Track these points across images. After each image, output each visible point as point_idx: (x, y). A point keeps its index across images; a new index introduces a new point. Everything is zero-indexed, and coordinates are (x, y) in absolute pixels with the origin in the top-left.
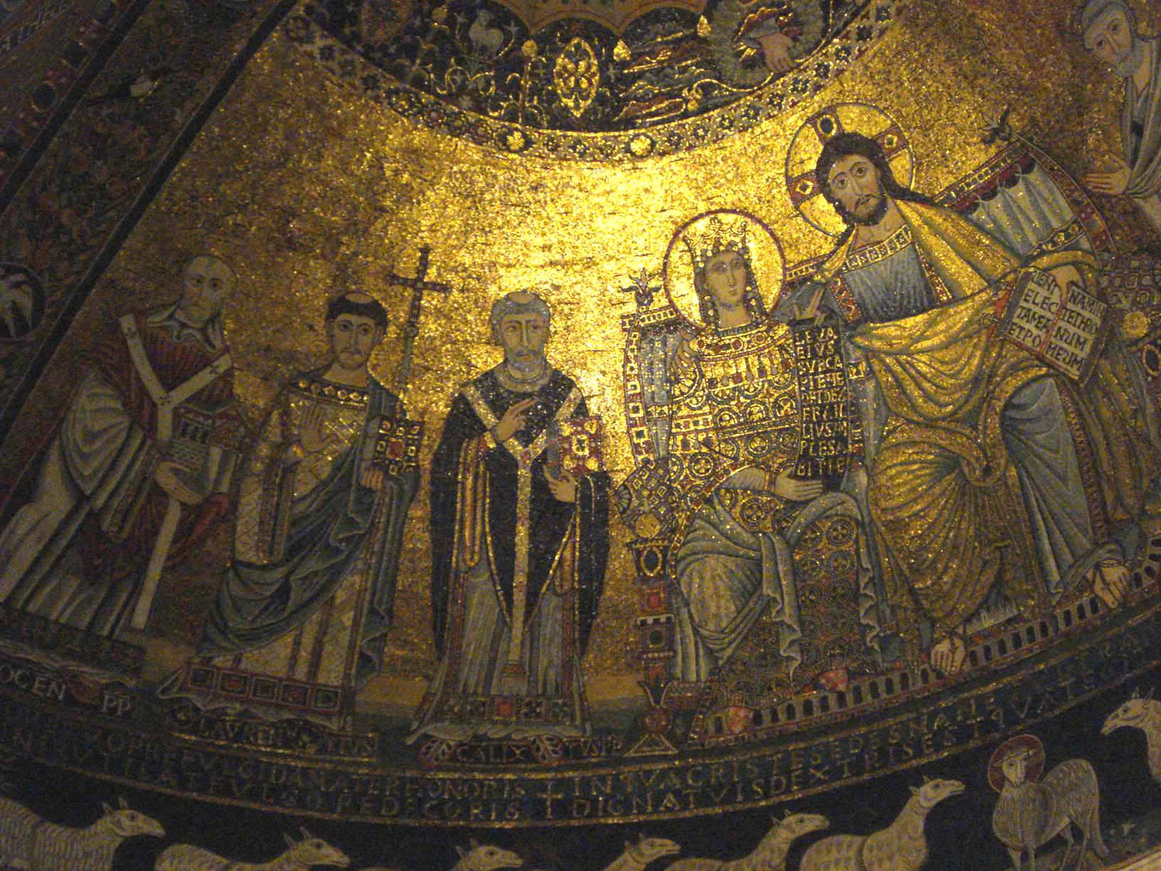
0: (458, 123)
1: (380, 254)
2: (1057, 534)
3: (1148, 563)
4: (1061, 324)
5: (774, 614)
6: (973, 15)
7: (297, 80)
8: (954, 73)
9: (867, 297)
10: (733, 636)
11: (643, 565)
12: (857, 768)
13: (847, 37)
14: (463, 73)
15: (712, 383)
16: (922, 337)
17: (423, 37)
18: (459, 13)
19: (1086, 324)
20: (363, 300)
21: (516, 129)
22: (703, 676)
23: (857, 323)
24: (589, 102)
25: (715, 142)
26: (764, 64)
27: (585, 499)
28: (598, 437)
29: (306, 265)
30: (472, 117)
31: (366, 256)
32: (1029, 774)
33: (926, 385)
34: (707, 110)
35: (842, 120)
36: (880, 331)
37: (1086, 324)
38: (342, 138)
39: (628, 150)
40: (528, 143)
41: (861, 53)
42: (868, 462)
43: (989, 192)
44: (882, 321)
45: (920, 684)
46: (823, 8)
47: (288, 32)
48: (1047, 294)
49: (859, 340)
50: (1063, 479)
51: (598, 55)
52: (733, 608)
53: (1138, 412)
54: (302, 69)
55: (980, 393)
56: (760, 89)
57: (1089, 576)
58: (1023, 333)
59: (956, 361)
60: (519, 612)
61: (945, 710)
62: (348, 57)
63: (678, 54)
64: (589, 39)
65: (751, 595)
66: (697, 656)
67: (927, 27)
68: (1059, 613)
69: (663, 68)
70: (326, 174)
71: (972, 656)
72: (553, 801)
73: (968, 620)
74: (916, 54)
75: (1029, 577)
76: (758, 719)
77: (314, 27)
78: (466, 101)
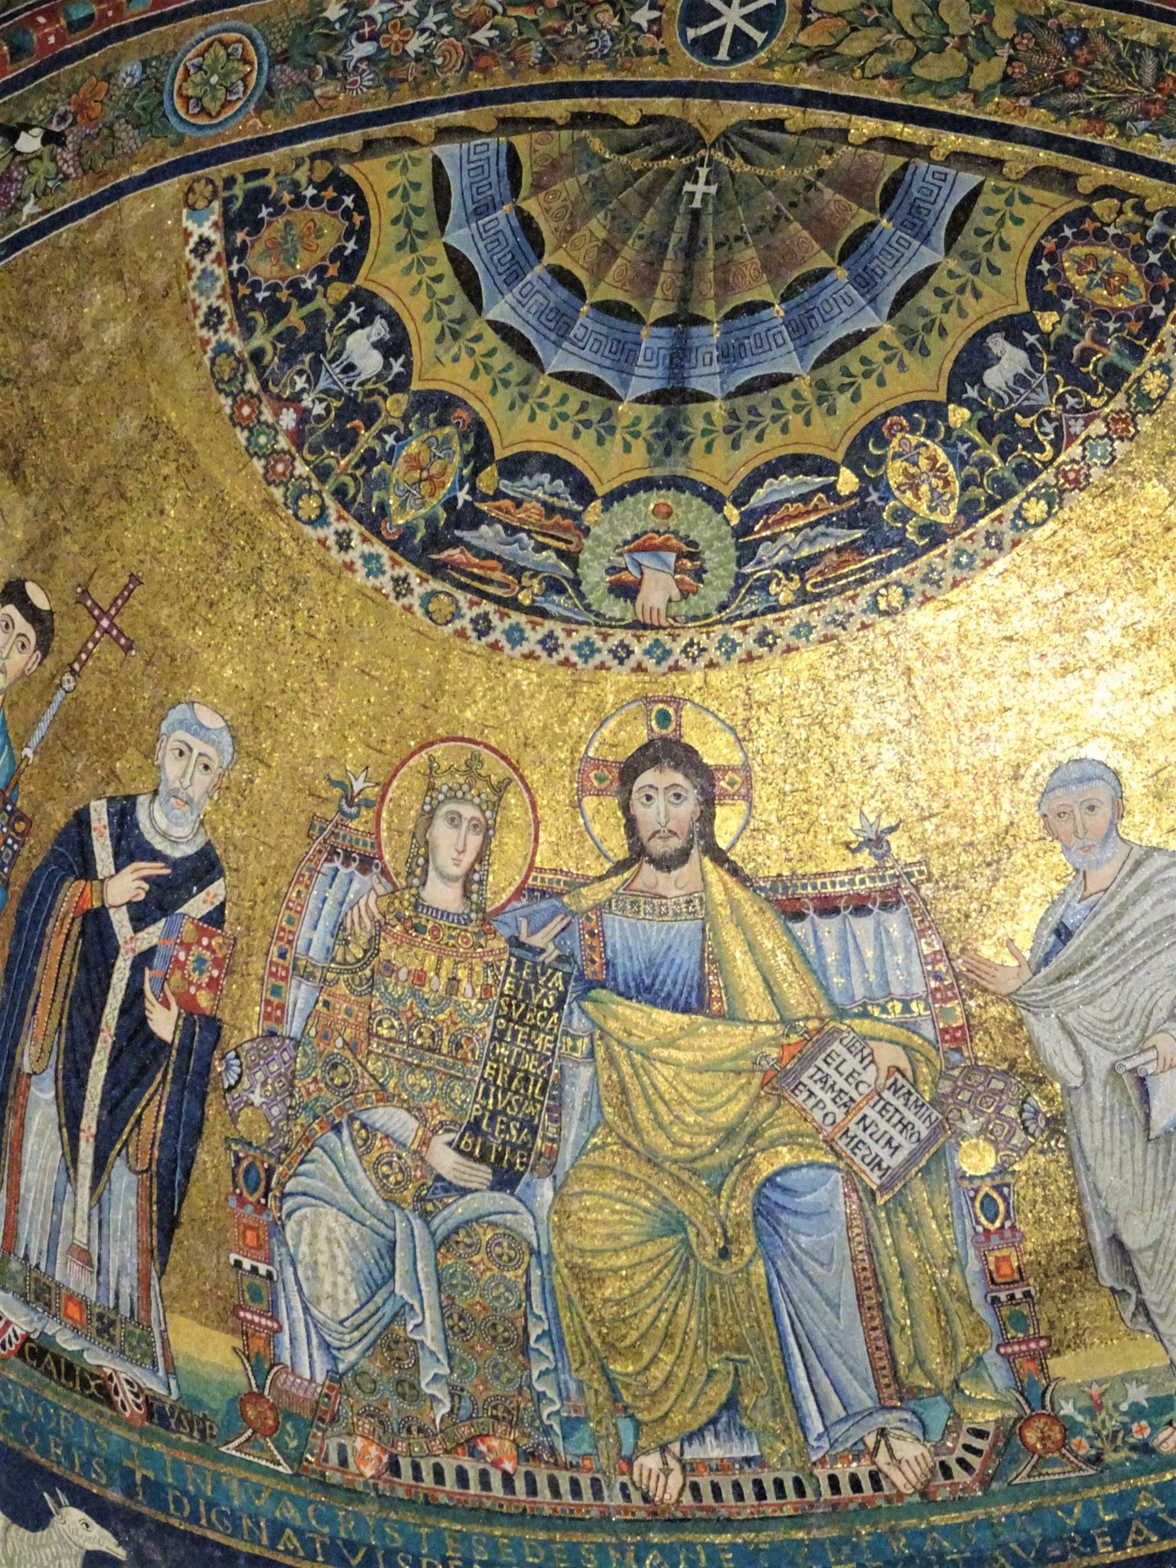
2: (819, 1371)
3: (960, 1453)
4: (867, 1111)
5: (410, 1327)
10: (356, 1335)
11: (240, 1179)
15: (390, 969)
16: (671, 1043)
19: (905, 1126)
22: (320, 1378)
23: (591, 985)
27: (185, 1049)
28: (227, 966)
30: (283, 443)
33: (661, 1108)
36: (620, 1009)
37: (905, 1126)
42: (558, 1171)
43: (828, 907)
44: (620, 994)
45: (619, 1500)
48: (859, 1068)
49: (589, 1006)
50: (835, 1307)
52: (354, 1296)
55: (735, 1150)
57: (871, 1441)
58: (812, 1101)
59: (711, 1095)
60: (85, 1170)
61: (661, 1547)
62: (219, 271)
64: (464, 437)
65: (379, 1288)
66: (309, 1343)
68: (822, 1474)
71: (695, 1489)
72: (145, 1478)
73: (690, 1438)
75: (777, 1413)
76: (394, 1467)
77: (216, 205)
78: (288, 419)
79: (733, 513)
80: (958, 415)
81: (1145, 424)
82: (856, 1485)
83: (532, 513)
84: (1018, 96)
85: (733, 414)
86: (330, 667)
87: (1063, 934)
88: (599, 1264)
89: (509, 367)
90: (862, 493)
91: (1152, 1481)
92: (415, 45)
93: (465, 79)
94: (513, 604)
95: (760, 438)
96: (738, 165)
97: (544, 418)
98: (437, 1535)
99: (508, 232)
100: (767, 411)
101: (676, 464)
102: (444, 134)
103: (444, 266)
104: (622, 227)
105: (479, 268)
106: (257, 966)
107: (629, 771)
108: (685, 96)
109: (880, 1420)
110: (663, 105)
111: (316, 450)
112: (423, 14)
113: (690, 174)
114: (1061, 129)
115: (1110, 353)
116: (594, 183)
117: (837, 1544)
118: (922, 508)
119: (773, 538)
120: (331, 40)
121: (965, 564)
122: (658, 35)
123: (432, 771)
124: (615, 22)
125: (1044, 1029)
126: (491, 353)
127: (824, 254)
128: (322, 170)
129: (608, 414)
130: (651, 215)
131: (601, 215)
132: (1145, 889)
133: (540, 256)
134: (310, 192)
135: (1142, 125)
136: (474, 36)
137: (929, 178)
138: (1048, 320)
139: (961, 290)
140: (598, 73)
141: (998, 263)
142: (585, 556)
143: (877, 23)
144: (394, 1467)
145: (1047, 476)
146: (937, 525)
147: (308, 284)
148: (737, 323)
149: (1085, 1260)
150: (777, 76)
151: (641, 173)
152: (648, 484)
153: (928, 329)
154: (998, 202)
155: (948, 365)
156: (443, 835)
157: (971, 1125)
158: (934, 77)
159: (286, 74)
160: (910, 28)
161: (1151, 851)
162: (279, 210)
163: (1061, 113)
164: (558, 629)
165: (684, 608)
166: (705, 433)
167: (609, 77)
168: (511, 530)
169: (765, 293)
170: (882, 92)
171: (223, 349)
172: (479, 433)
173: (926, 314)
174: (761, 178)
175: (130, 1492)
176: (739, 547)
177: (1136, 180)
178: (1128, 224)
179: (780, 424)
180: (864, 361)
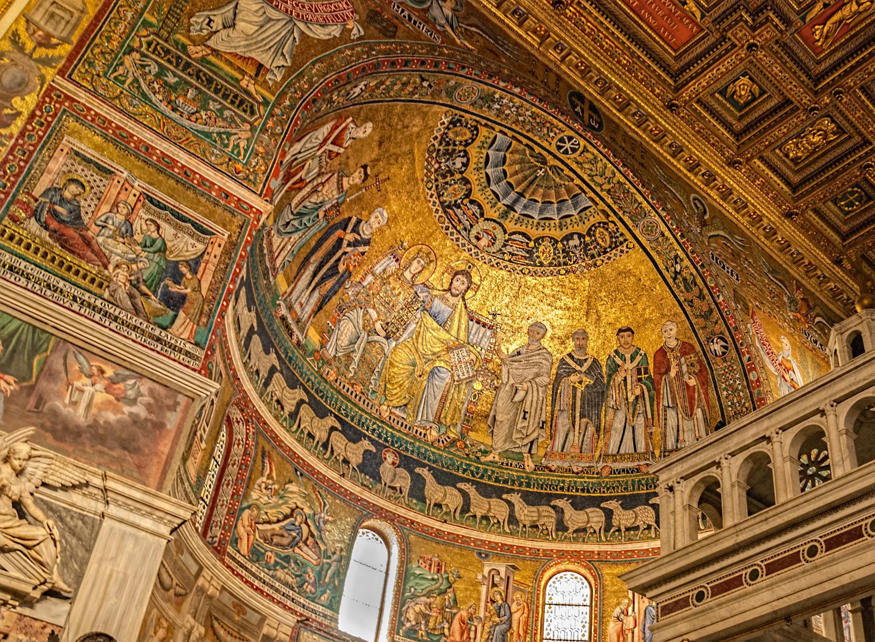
9: (434, 309)
12: (352, 420)
16: (433, 330)
19: (468, 372)
30: (433, 170)
32: (393, 464)
37: (468, 372)
41: (493, 266)
43: (478, 322)
53: (463, 403)
55: (434, 357)
73: (394, 407)
75: (413, 412)
78: (437, 166)
79: (507, 237)
80: (560, 245)
81: (593, 269)
82: (420, 434)
83: (470, 213)
86: (414, 218)
87: (519, 353)
88: (396, 364)
91: (476, 465)
92: (507, 112)
94: (456, 228)
96: (550, 173)
97: (484, 196)
98: (337, 399)
100: (526, 222)
102: (501, 132)
103: (484, 156)
104: (522, 170)
106: (365, 268)
107: (456, 274)
109: (432, 424)
110: (545, 153)
113: (541, 169)
114: (613, 206)
115: (595, 252)
117: (411, 443)
118: (542, 258)
120: (492, 101)
121: (543, 274)
123: (420, 250)
125: (504, 369)
128: (474, 123)
129: (496, 203)
130: (528, 172)
132: (539, 354)
138: (587, 239)
140: (536, 139)
144: (336, 381)
145: (569, 267)
149: (487, 417)
150: (569, 162)
152: (495, 221)
154: (593, 211)
156: (415, 263)
157: (480, 379)
159: (480, 102)
161: (544, 348)
163: (615, 203)
164: (461, 238)
168: (464, 213)
169: (539, 199)
170: (585, 177)
171: (434, 145)
172: (470, 191)
175: (286, 357)
177: (619, 224)
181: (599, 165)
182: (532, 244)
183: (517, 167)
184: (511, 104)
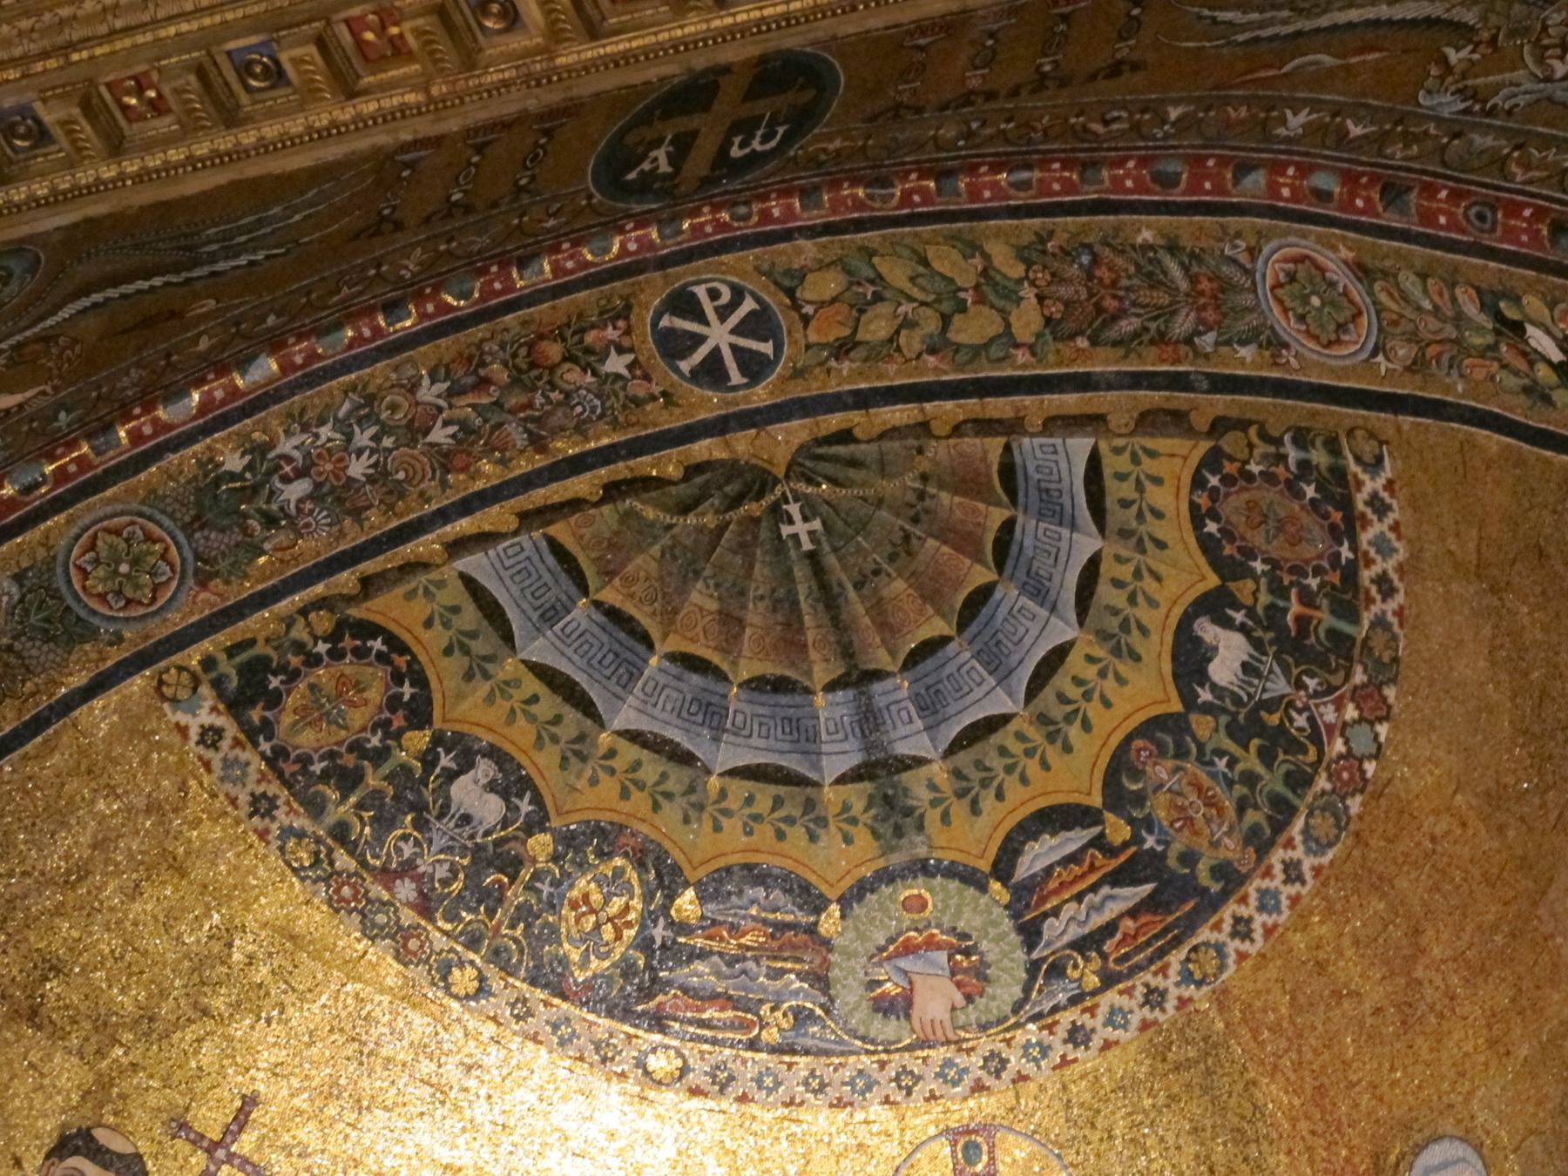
0: (381, 919)
1: (175, 1080)
6: (1254, 1083)
7: (145, 761)
8: (1197, 1157)
13: (1050, 1028)
14: (417, 843)
17: (376, 766)
18: (448, 752)
20: (117, 1144)
21: (472, 963)
24: (606, 964)
25: (786, 1105)
26: (908, 1017)
29: (49, 1057)
30: (408, 917)
31: (151, 1076)
34: (792, 1051)
35: (998, 1154)
38: (183, 873)
39: (641, 1064)
40: (482, 990)
41: (1065, 1062)
46: (1028, 971)
47: (161, 682)
51: (648, 897)
54: (159, 746)
56: (887, 1051)
62: (246, 755)
63: (775, 944)
64: (641, 865)
67: (1177, 1068)
69: (744, 959)
70: (135, 924)
74: (1147, 1102)
77: (205, 690)
78: (406, 890)
84: (1072, 337)
85: (957, 774)
89: (664, 776)
90: (1137, 839)
92: (357, 469)
93: (444, 484)
95: (1000, 796)
99: (596, 630)
100: (997, 763)
101: (913, 844)
102: (457, 547)
103: (532, 685)
105: (579, 677)
108: (722, 433)
110: (703, 449)
111: (452, 917)
112: (349, 437)
113: (777, 513)
116: (669, 553)
119: (1055, 912)
122: (647, 378)
124: (589, 379)
126: (636, 766)
127: (978, 567)
128: (323, 622)
129: (810, 805)
131: (700, 585)
133: (650, 646)
134: (322, 647)
135: (1210, 337)
136: (429, 439)
137: (1039, 454)
138: (1243, 589)
139: (1137, 575)
141: (1160, 535)
142: (835, 973)
143: (878, 298)
145: (1322, 783)
146: (1229, 863)
147: (375, 741)
148: (923, 668)
151: (722, 529)
152: (887, 877)
153: (1125, 626)
155: (1167, 667)
158: (977, 340)
159: (215, 541)
160: (916, 293)
162: (294, 676)
165: (972, 1014)
166: (934, 803)
167: (617, 438)
169: (938, 627)
170: (935, 369)
173: (1115, 612)
174: (864, 499)
176: (1021, 929)
178: (1265, 456)
179: (1016, 775)
180: (1078, 681)
181: (897, 273)
182: (1118, 830)
183: (701, 598)
184: (325, 432)
